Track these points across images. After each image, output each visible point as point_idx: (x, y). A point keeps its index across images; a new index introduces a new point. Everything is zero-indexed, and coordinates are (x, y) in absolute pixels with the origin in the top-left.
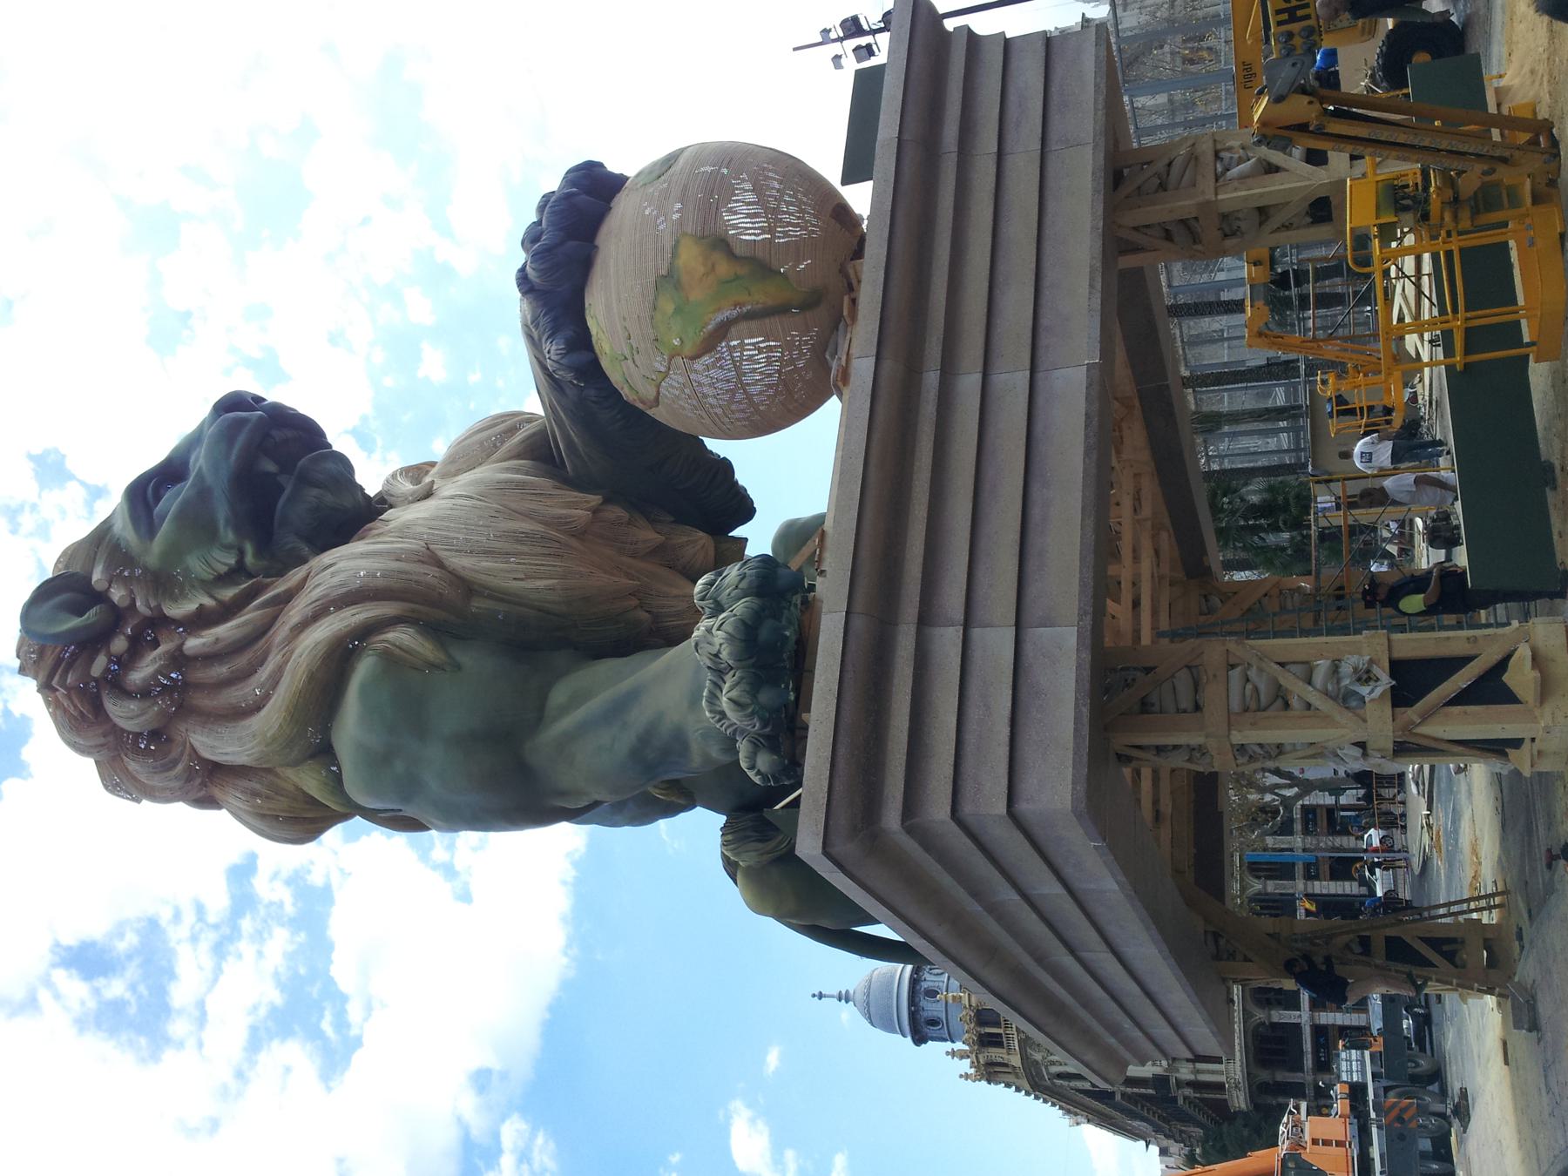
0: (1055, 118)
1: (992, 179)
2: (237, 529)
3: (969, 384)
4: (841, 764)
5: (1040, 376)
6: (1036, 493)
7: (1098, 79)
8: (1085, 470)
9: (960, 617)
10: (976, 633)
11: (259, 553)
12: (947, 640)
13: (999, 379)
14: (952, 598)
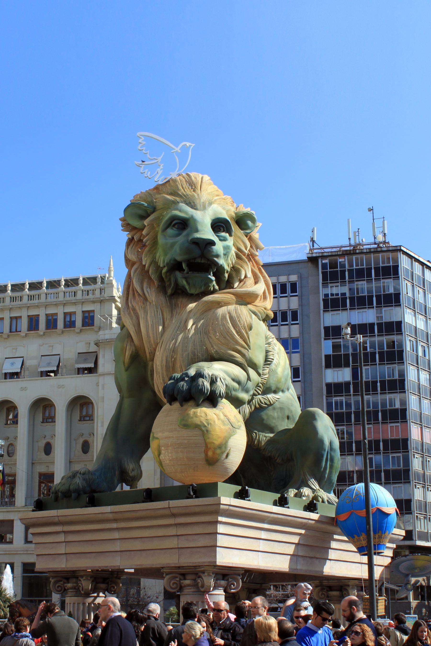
1: (169, 534)
2: (167, 264)
3: (116, 535)
4: (34, 519)
5: (119, 553)
9: (66, 541)
10: (64, 544)
11: (167, 272)
12: (61, 538)
13: (118, 542)
14: (71, 538)
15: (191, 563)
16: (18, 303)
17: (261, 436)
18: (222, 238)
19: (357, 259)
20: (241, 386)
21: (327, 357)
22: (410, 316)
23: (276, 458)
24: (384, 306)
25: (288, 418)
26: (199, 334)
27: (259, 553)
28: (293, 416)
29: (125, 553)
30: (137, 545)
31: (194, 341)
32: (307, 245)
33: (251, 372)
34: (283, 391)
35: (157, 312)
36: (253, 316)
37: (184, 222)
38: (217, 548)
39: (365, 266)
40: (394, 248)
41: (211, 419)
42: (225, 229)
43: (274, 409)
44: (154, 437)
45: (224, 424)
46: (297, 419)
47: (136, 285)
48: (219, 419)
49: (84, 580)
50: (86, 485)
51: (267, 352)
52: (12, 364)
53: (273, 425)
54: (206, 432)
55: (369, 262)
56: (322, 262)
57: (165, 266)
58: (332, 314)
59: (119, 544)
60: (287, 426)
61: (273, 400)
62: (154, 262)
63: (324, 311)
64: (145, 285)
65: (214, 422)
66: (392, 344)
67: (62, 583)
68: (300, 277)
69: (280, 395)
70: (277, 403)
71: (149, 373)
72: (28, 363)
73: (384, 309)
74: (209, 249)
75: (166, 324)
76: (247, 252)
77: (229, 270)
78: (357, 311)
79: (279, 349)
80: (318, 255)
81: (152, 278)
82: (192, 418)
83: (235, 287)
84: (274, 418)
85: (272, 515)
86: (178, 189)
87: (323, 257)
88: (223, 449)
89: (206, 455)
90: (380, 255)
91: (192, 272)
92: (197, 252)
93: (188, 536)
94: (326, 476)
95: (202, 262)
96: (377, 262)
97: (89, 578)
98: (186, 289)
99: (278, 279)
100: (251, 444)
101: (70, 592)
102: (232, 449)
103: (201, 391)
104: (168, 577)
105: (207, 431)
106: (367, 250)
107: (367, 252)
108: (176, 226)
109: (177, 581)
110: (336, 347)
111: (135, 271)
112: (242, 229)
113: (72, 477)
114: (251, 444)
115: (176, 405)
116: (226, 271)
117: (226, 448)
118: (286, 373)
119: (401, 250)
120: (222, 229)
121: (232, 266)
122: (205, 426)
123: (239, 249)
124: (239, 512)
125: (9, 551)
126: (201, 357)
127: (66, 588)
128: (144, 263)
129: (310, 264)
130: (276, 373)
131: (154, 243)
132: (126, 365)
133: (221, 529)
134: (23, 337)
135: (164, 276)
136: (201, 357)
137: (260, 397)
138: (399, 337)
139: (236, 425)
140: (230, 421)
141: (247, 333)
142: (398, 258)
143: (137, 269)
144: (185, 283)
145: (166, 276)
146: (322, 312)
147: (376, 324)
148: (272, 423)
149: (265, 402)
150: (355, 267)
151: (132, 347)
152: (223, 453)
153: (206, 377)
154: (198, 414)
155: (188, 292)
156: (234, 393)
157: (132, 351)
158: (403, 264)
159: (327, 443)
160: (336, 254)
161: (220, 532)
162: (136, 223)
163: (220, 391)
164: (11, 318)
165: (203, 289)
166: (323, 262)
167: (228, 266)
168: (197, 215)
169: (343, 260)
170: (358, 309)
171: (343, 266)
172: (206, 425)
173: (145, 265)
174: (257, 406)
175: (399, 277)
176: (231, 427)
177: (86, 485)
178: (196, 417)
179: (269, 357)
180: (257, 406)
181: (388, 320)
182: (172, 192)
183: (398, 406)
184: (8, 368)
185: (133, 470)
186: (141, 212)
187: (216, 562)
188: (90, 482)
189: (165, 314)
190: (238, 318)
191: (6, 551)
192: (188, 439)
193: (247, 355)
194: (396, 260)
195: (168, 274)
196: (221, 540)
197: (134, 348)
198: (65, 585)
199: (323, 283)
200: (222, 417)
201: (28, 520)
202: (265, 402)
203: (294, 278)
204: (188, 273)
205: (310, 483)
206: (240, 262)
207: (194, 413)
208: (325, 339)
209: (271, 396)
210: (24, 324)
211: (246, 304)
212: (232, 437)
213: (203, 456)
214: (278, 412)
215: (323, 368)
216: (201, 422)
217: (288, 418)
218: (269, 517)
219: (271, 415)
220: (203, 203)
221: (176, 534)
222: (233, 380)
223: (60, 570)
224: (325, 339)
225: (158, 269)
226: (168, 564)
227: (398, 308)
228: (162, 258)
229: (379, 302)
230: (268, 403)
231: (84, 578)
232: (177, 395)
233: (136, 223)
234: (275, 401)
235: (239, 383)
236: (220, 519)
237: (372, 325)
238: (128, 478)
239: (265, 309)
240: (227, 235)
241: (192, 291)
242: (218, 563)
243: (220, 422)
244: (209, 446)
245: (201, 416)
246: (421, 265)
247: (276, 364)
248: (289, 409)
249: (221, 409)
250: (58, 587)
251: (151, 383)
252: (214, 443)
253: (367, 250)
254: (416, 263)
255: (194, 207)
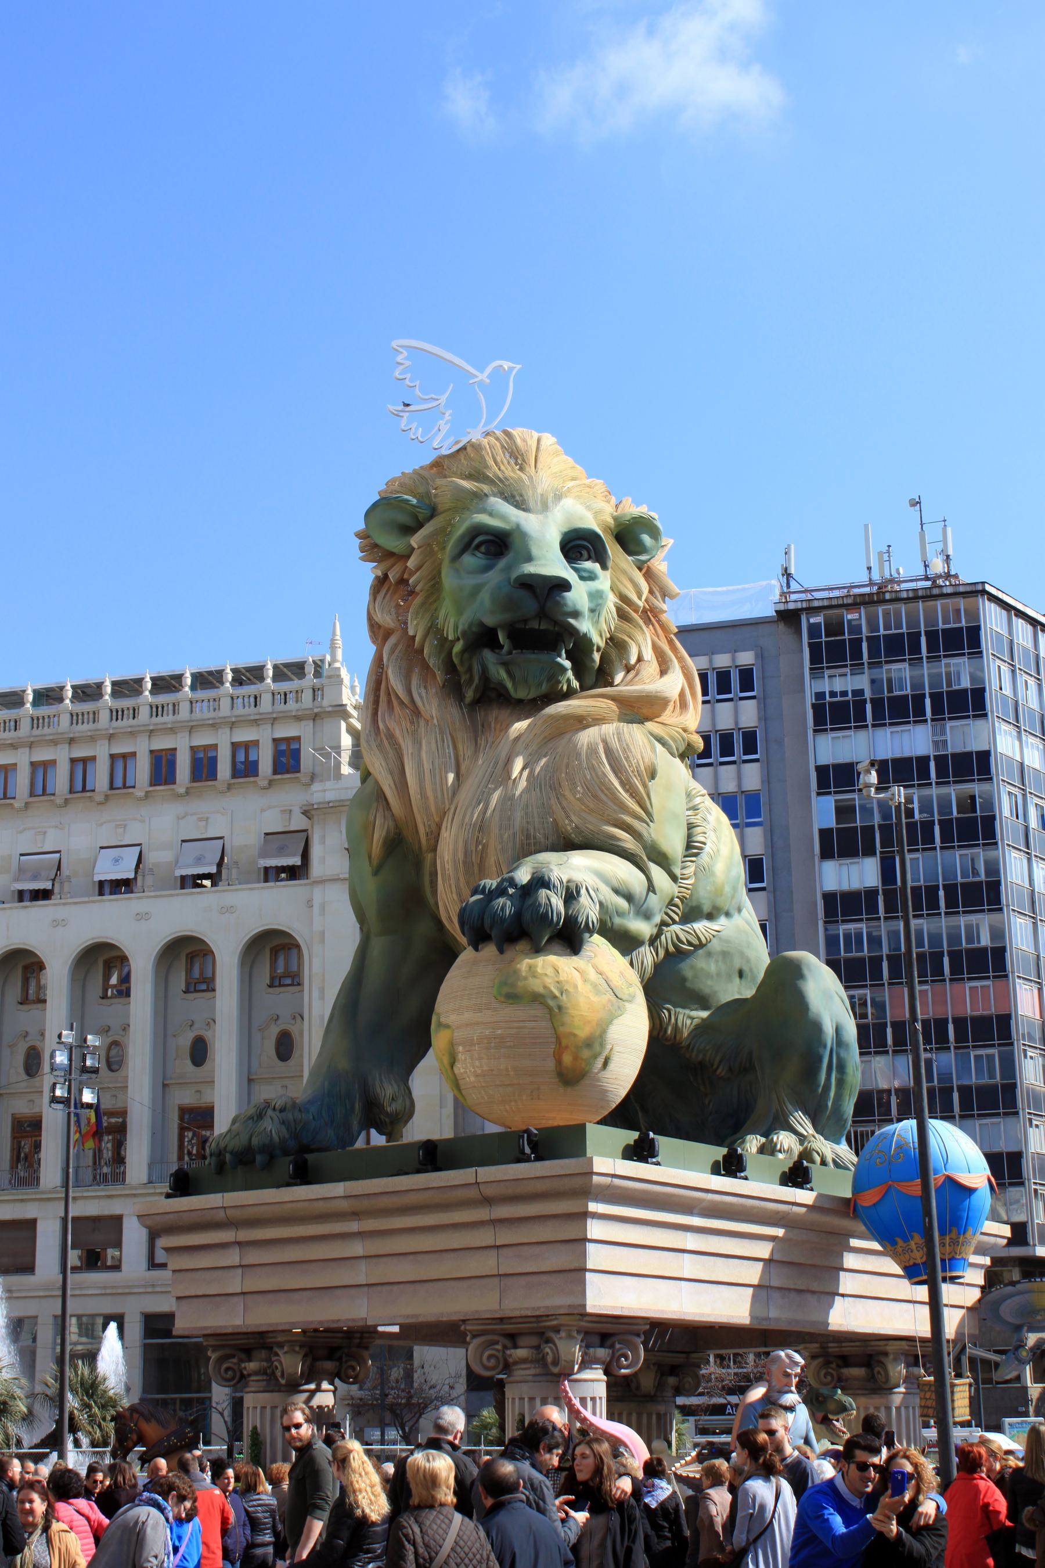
0: (522, 1280)
2: (464, 633)
3: (357, 1248)
4: (171, 1216)
5: (366, 1289)
6: (309, 1293)
7: (542, 1310)
8: (312, 1322)
9: (243, 1263)
10: (239, 1271)
11: (463, 652)
12: (233, 1257)
13: (363, 1266)
14: (254, 1257)
15: (527, 1309)
16: (127, 722)
17: (680, 1017)
18: (585, 574)
19: (887, 614)
20: (634, 905)
21: (825, 834)
22: (1009, 738)
23: (715, 1067)
24: (950, 719)
25: (741, 974)
26: (538, 790)
27: (682, 1282)
28: (751, 970)
29: (379, 1288)
30: (405, 1271)
31: (527, 805)
32: (776, 585)
33: (657, 873)
34: (728, 914)
35: (443, 741)
36: (659, 747)
37: (499, 539)
38: (588, 1275)
39: (904, 630)
40: (969, 589)
41: (567, 982)
42: (593, 554)
43: (709, 954)
44: (440, 1025)
45: (597, 992)
46: (761, 975)
47: (395, 681)
48: (585, 981)
49: (286, 1353)
50: (287, 1136)
51: (691, 827)
52: (116, 860)
53: (707, 991)
54: (557, 1011)
55: (913, 622)
56: (808, 621)
57: (458, 639)
58: (833, 738)
59: (364, 1269)
60: (739, 993)
61: (707, 935)
62: (433, 629)
63: (815, 731)
64: (415, 681)
65: (576, 987)
66: (969, 803)
67: (235, 1360)
68: (761, 656)
69: (721, 924)
70: (714, 941)
71: (427, 879)
72: (152, 858)
73: (949, 724)
74: (558, 598)
75: (463, 768)
76: (641, 604)
77: (602, 644)
78: (889, 730)
79: (718, 820)
80: (799, 605)
81: (431, 665)
82: (526, 978)
83: (616, 683)
84: (709, 975)
85: (710, 1196)
86: (487, 467)
87: (812, 610)
88: (597, 1047)
89: (559, 1061)
90: (939, 604)
91: (520, 651)
92: (530, 606)
93: (520, 1247)
94: (830, 1104)
95: (542, 627)
96: (931, 619)
97: (297, 1349)
98: (506, 689)
99: (711, 661)
100: (658, 1034)
101: (253, 1381)
102: (616, 1049)
103: (544, 918)
104: (476, 1342)
105: (560, 1008)
106: (910, 592)
107: (908, 599)
108: (483, 549)
109: (498, 1350)
110: (844, 811)
111: (392, 651)
112: (629, 553)
113: (255, 1118)
114: (658, 1034)
115: (490, 950)
116: (595, 648)
117: (602, 1045)
118: (734, 873)
119: (984, 592)
120: (585, 553)
121: (608, 636)
122: (555, 997)
123: (623, 598)
124: (635, 1190)
125: (113, 1287)
126: (542, 840)
127: (245, 1373)
128: (411, 633)
129: (781, 626)
130: (713, 874)
131: (434, 585)
132: (375, 863)
133: (595, 1229)
134: (140, 799)
135: (456, 660)
136: (542, 840)
137: (676, 928)
138: (985, 786)
139: (624, 992)
140: (611, 983)
141: (645, 786)
142: (978, 609)
143: (396, 645)
144: (503, 674)
145: (462, 662)
146: (810, 732)
147: (932, 758)
148: (706, 986)
149: (687, 940)
150: (882, 632)
151: (386, 822)
152: (596, 1056)
153: (554, 886)
154: (539, 970)
155: (510, 695)
156: (617, 921)
157: (388, 832)
158: (991, 624)
159: (829, 1029)
160: (840, 602)
161: (594, 1237)
162: (392, 542)
163: (587, 918)
164: (113, 757)
165: (544, 688)
166: (812, 621)
167: (601, 636)
168: (529, 522)
169: (855, 616)
170: (891, 724)
171: (856, 629)
172: (557, 994)
173: (414, 637)
174: (671, 949)
175: (981, 652)
176: (614, 998)
177: (287, 1136)
178: (534, 977)
179: (695, 839)
180: (671, 949)
181: (959, 749)
182: (473, 472)
183: (985, 941)
184: (108, 870)
185: (393, 1099)
186: (403, 518)
187: (584, 1306)
188: (296, 1129)
189: (460, 746)
190: (624, 751)
191: (105, 1288)
192: (517, 1028)
193: (645, 834)
194: (974, 615)
195: (466, 656)
196: (596, 1256)
197: (391, 823)
198: (243, 1365)
199: (811, 669)
200: (592, 975)
201: (155, 1217)
202: (687, 940)
203: (746, 658)
204: (510, 653)
205: (792, 1121)
206: (626, 626)
207: (530, 967)
208: (819, 794)
209: (701, 927)
210: (142, 769)
211: (641, 720)
212: (615, 1022)
213: (551, 1064)
214: (717, 961)
215: (817, 859)
216: (545, 987)
217: (741, 974)
218: (701, 1200)
219: (702, 969)
220: (542, 495)
221: (493, 1244)
222: (617, 891)
223: (230, 1330)
224: (819, 794)
225: (444, 644)
226: (477, 1311)
227: (980, 723)
228: (452, 621)
229: (937, 710)
230: (695, 942)
231: (286, 1349)
232: (491, 928)
233: (392, 542)
234: (711, 936)
235: (629, 897)
236: (593, 1207)
237: (923, 761)
238: (382, 1117)
239: (685, 730)
240: (597, 566)
241: (522, 694)
242: (589, 1309)
243: (589, 987)
244: (564, 1042)
245: (546, 974)
246: (1031, 624)
247: (712, 853)
248: (742, 954)
249: (591, 958)
250: (227, 1369)
251: (431, 901)
252: (575, 1035)
253: (910, 592)
254: (1020, 621)
255: (521, 504)
